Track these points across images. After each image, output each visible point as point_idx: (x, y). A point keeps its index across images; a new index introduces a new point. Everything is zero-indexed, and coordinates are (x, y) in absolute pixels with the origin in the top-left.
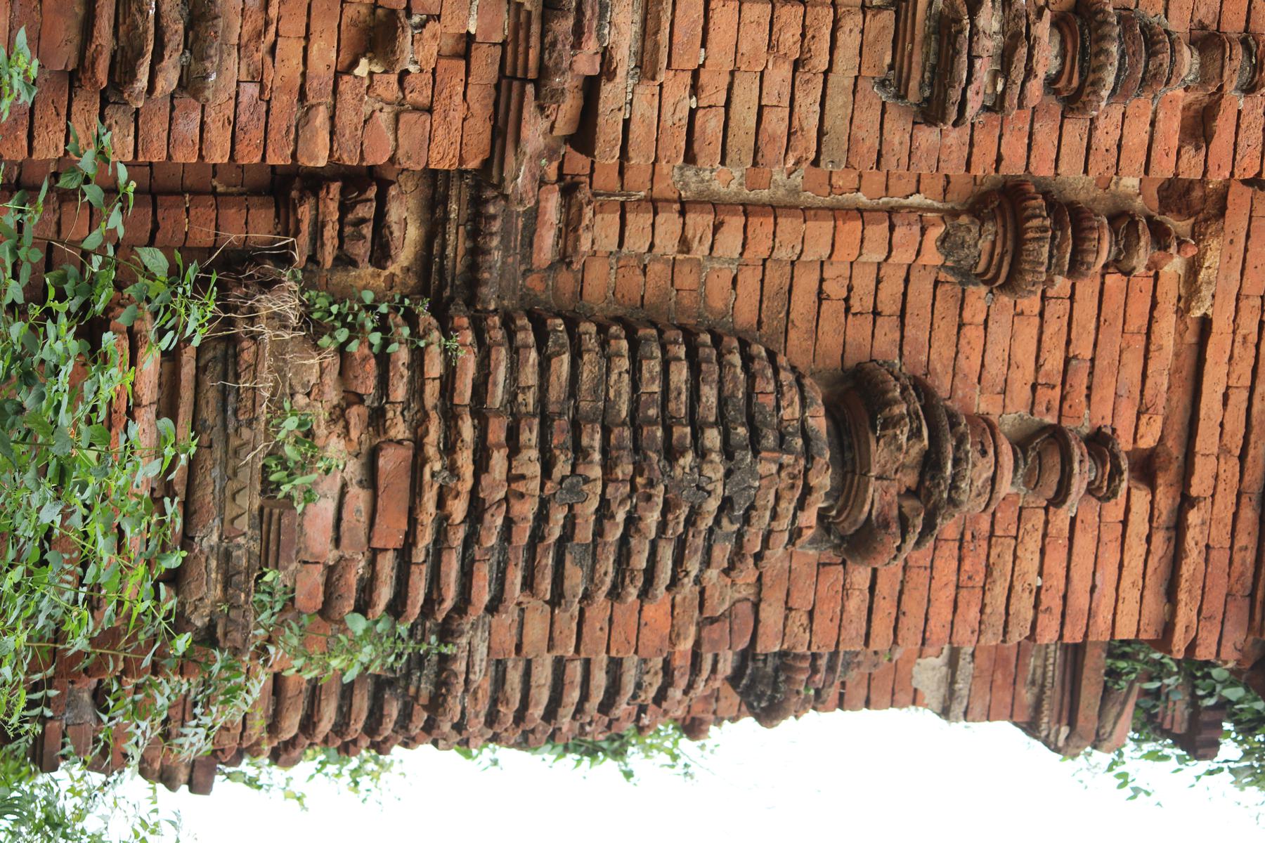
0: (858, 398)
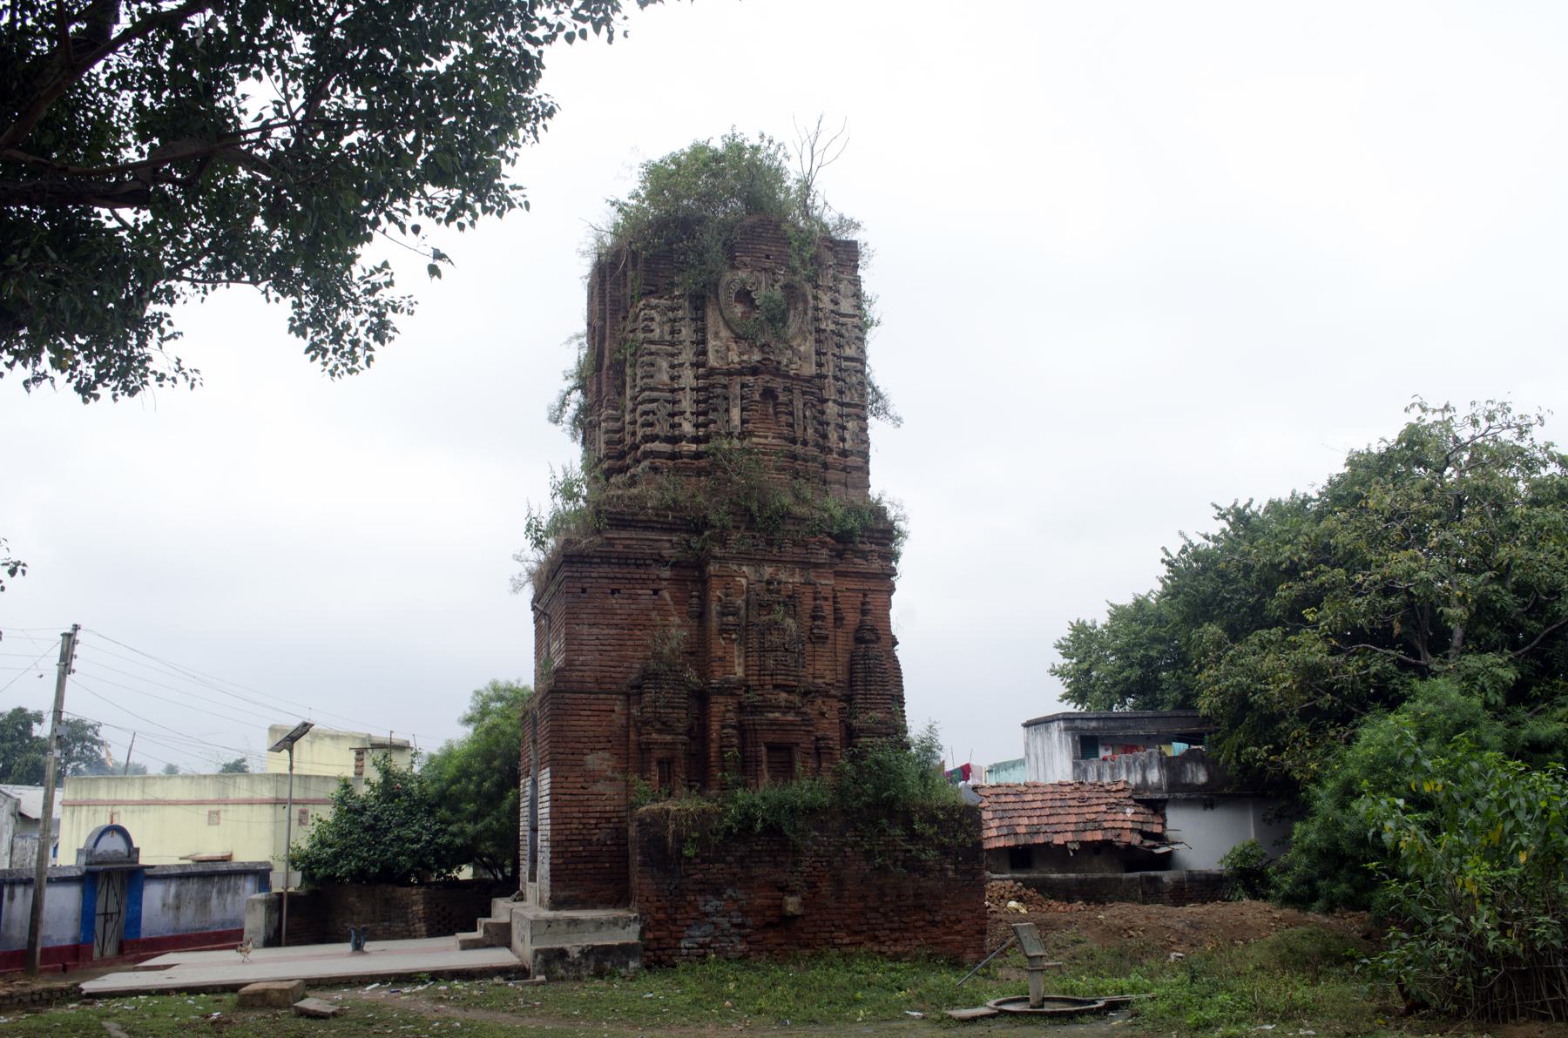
0: (859, 640)
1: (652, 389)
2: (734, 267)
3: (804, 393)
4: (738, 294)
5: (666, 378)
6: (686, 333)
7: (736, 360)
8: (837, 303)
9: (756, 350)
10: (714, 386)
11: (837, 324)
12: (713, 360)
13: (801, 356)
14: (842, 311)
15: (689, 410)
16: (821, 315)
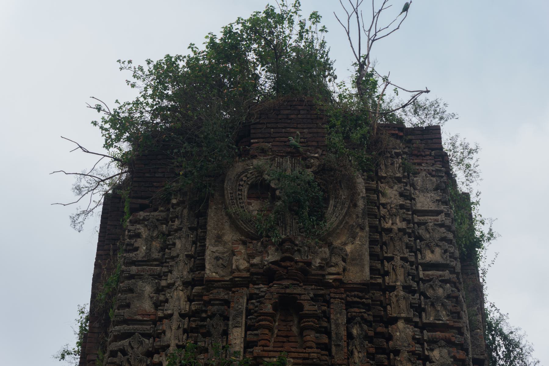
1: (126, 322)
2: (245, 155)
3: (349, 305)
4: (252, 187)
5: (148, 306)
6: (181, 246)
7: (244, 265)
8: (412, 199)
9: (271, 250)
10: (208, 303)
11: (409, 222)
12: (210, 272)
13: (350, 257)
14: (419, 206)
15: (173, 343)
16: (383, 211)
